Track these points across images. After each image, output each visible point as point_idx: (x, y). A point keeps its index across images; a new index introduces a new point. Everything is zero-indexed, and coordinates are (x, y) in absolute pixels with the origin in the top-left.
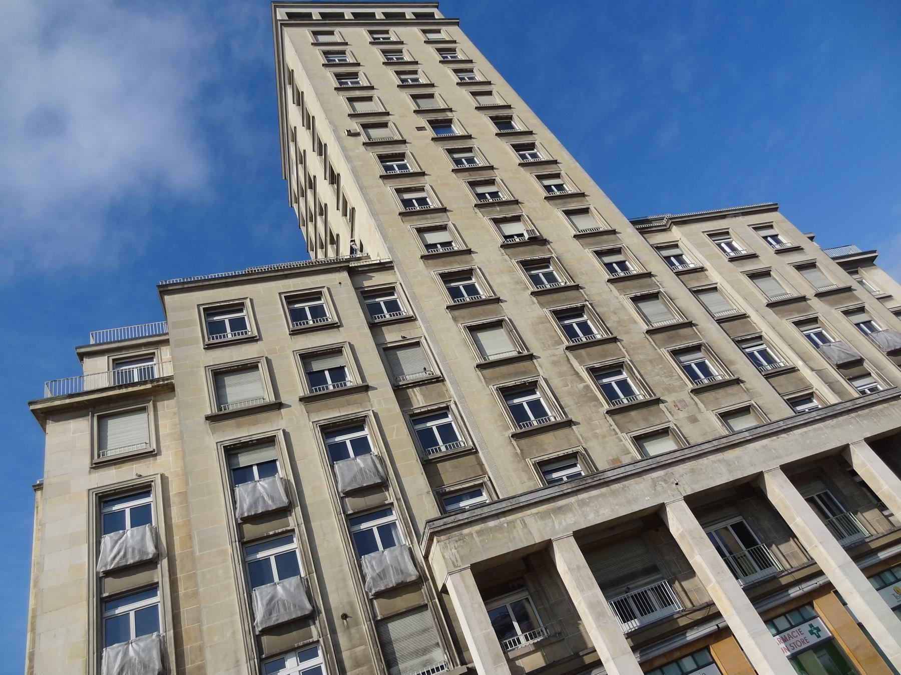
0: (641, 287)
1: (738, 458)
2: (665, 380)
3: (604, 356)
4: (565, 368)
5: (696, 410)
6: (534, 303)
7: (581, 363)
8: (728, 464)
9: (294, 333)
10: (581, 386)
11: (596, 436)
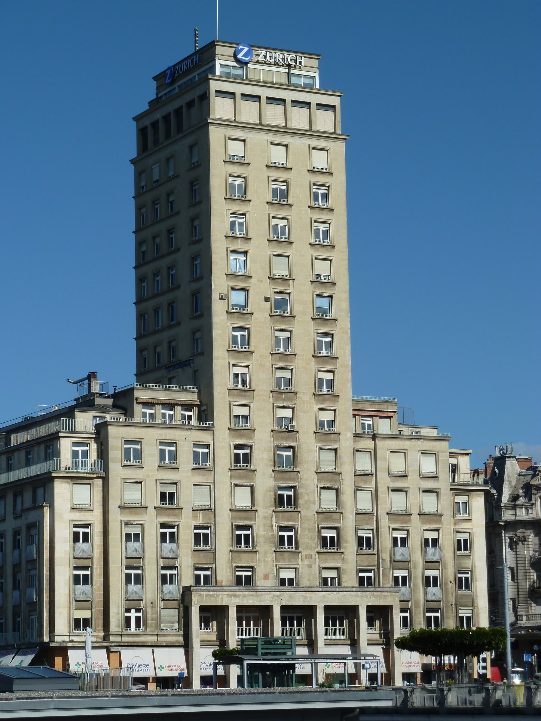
0: (331, 481)
1: (311, 597)
2: (309, 541)
3: (288, 520)
4: (269, 522)
5: (314, 562)
6: (271, 477)
7: (277, 521)
8: (305, 598)
9: (160, 467)
10: (271, 533)
11: (265, 561)
